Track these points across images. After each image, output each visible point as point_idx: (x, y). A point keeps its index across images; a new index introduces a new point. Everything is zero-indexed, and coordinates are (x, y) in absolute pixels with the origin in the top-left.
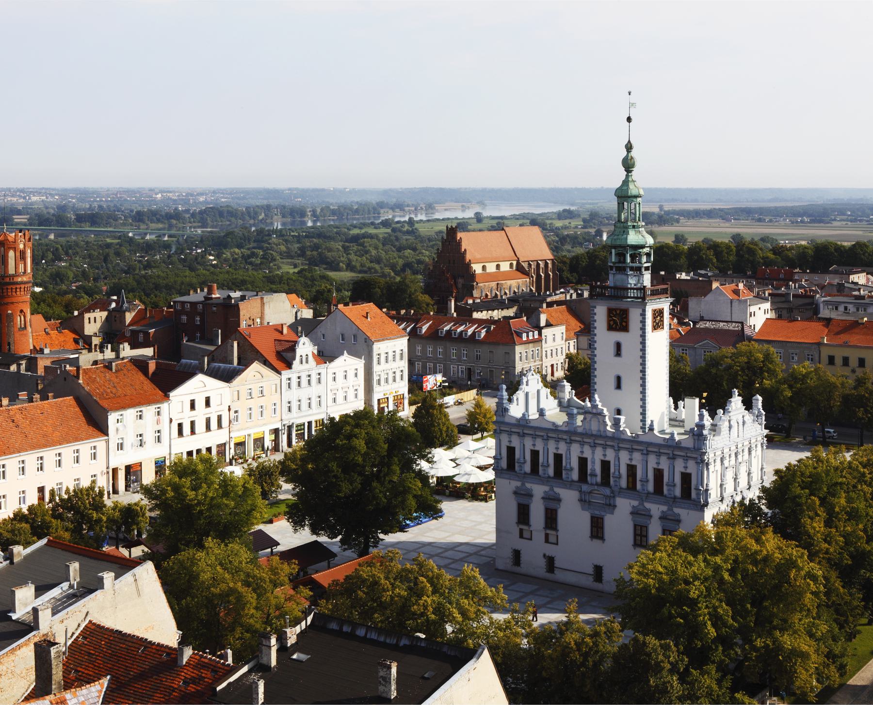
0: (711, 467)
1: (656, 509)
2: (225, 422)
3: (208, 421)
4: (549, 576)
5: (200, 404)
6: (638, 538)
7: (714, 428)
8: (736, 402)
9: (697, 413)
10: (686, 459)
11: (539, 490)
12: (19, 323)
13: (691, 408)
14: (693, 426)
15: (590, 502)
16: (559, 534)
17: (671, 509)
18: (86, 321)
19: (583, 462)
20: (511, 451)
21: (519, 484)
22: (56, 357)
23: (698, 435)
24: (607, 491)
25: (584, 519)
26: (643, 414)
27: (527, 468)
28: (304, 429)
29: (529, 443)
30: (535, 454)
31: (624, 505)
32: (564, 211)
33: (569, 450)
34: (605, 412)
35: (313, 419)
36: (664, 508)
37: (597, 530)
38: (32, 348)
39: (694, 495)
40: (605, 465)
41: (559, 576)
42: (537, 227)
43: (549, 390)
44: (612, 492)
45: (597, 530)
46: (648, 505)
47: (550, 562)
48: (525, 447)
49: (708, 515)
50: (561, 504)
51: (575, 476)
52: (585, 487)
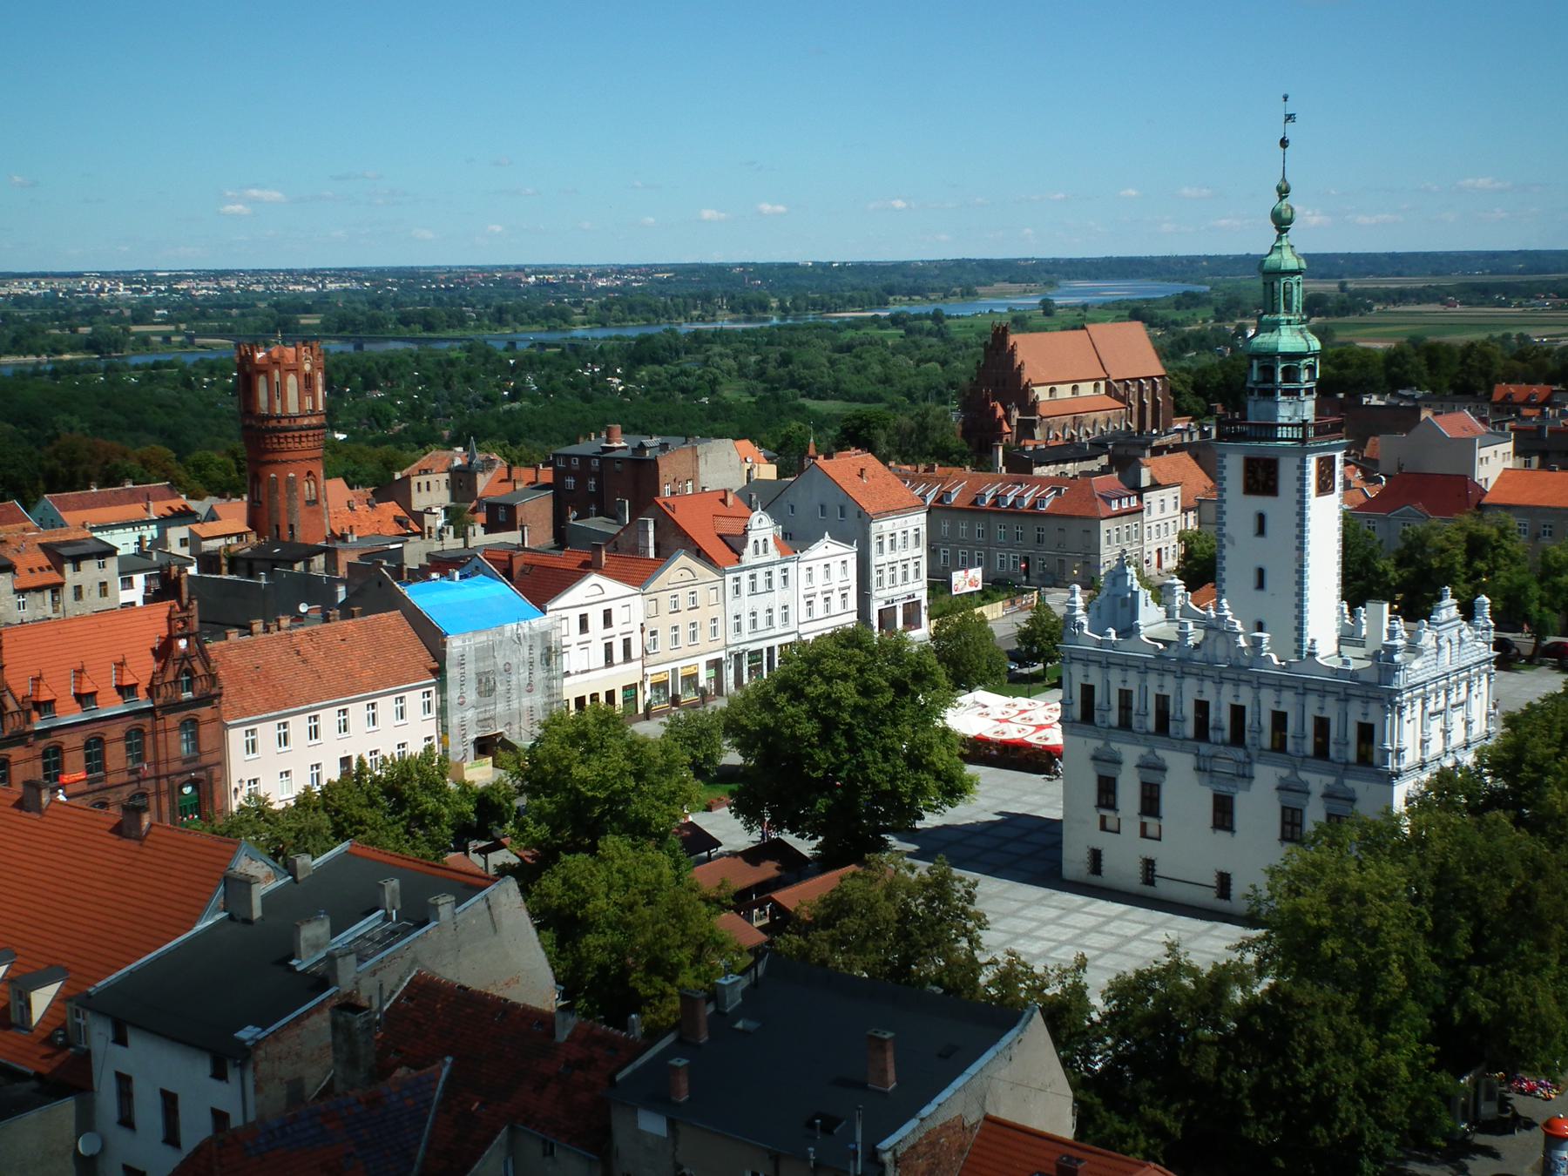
0: (1407, 714)
1: (1317, 782)
2: (636, 651)
3: (609, 648)
4: (1148, 890)
5: (595, 621)
6: (1288, 828)
7: (1413, 648)
8: (1448, 609)
9: (1386, 625)
10: (1366, 700)
11: (1131, 754)
12: (307, 493)
13: (1380, 619)
14: (1379, 648)
15: (1212, 771)
16: (1164, 823)
17: (1340, 781)
18: (414, 488)
19: (1202, 707)
20: (1088, 691)
21: (1099, 743)
22: (368, 547)
23: (1385, 662)
24: (1239, 754)
25: (1202, 800)
26: (1300, 629)
27: (1114, 718)
28: (761, 660)
29: (1115, 677)
30: (1125, 696)
31: (1267, 775)
32: (1186, 294)
33: (1180, 688)
34: (1239, 627)
35: (775, 642)
36: (1330, 780)
37: (1223, 815)
38: (328, 532)
39: (1377, 759)
40: (1238, 712)
41: (1162, 889)
42: (1139, 324)
43: (1150, 593)
44: (1249, 756)
45: (1223, 815)
46: (1303, 775)
47: (1149, 865)
48: (1109, 685)
49: (1401, 793)
50: (1167, 775)
51: (1189, 729)
52: (1204, 748)
